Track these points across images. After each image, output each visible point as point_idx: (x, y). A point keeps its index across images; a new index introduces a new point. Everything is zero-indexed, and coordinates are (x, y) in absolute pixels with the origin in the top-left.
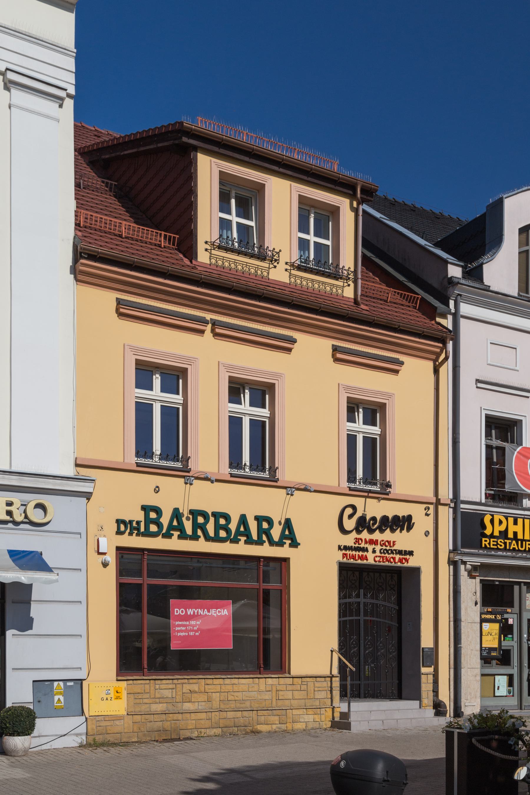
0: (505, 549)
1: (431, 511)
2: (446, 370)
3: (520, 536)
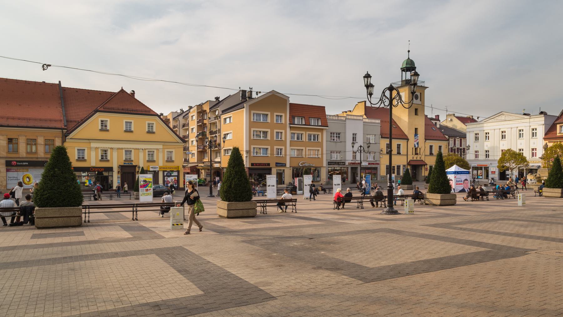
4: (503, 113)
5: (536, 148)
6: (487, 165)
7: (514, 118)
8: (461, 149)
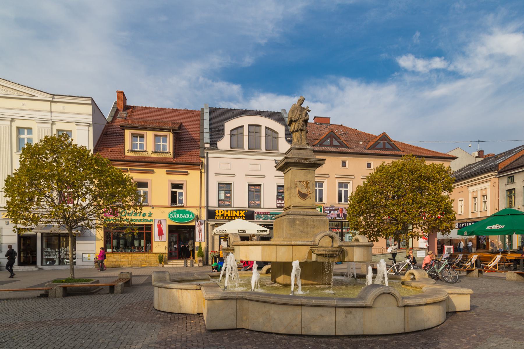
0: (224, 219)
1: (199, 210)
2: (204, 176)
3: (229, 215)
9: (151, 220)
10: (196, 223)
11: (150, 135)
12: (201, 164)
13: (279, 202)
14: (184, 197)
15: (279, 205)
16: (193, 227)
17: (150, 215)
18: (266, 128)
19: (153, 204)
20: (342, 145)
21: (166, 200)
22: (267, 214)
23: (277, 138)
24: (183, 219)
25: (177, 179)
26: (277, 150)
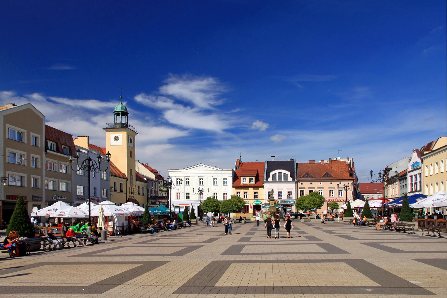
2: (264, 190)
4: (201, 164)
5: (226, 192)
6: (188, 205)
7: (210, 169)
8: (156, 191)
9: (248, 204)
10: (262, 204)
11: (248, 178)
12: (263, 186)
13: (288, 197)
14: (258, 196)
15: (289, 198)
16: (261, 205)
17: (248, 202)
18: (284, 173)
19: (249, 199)
20: (311, 177)
21: (253, 198)
22: (284, 201)
23: (287, 177)
24: (258, 203)
25: (256, 191)
26: (288, 180)
